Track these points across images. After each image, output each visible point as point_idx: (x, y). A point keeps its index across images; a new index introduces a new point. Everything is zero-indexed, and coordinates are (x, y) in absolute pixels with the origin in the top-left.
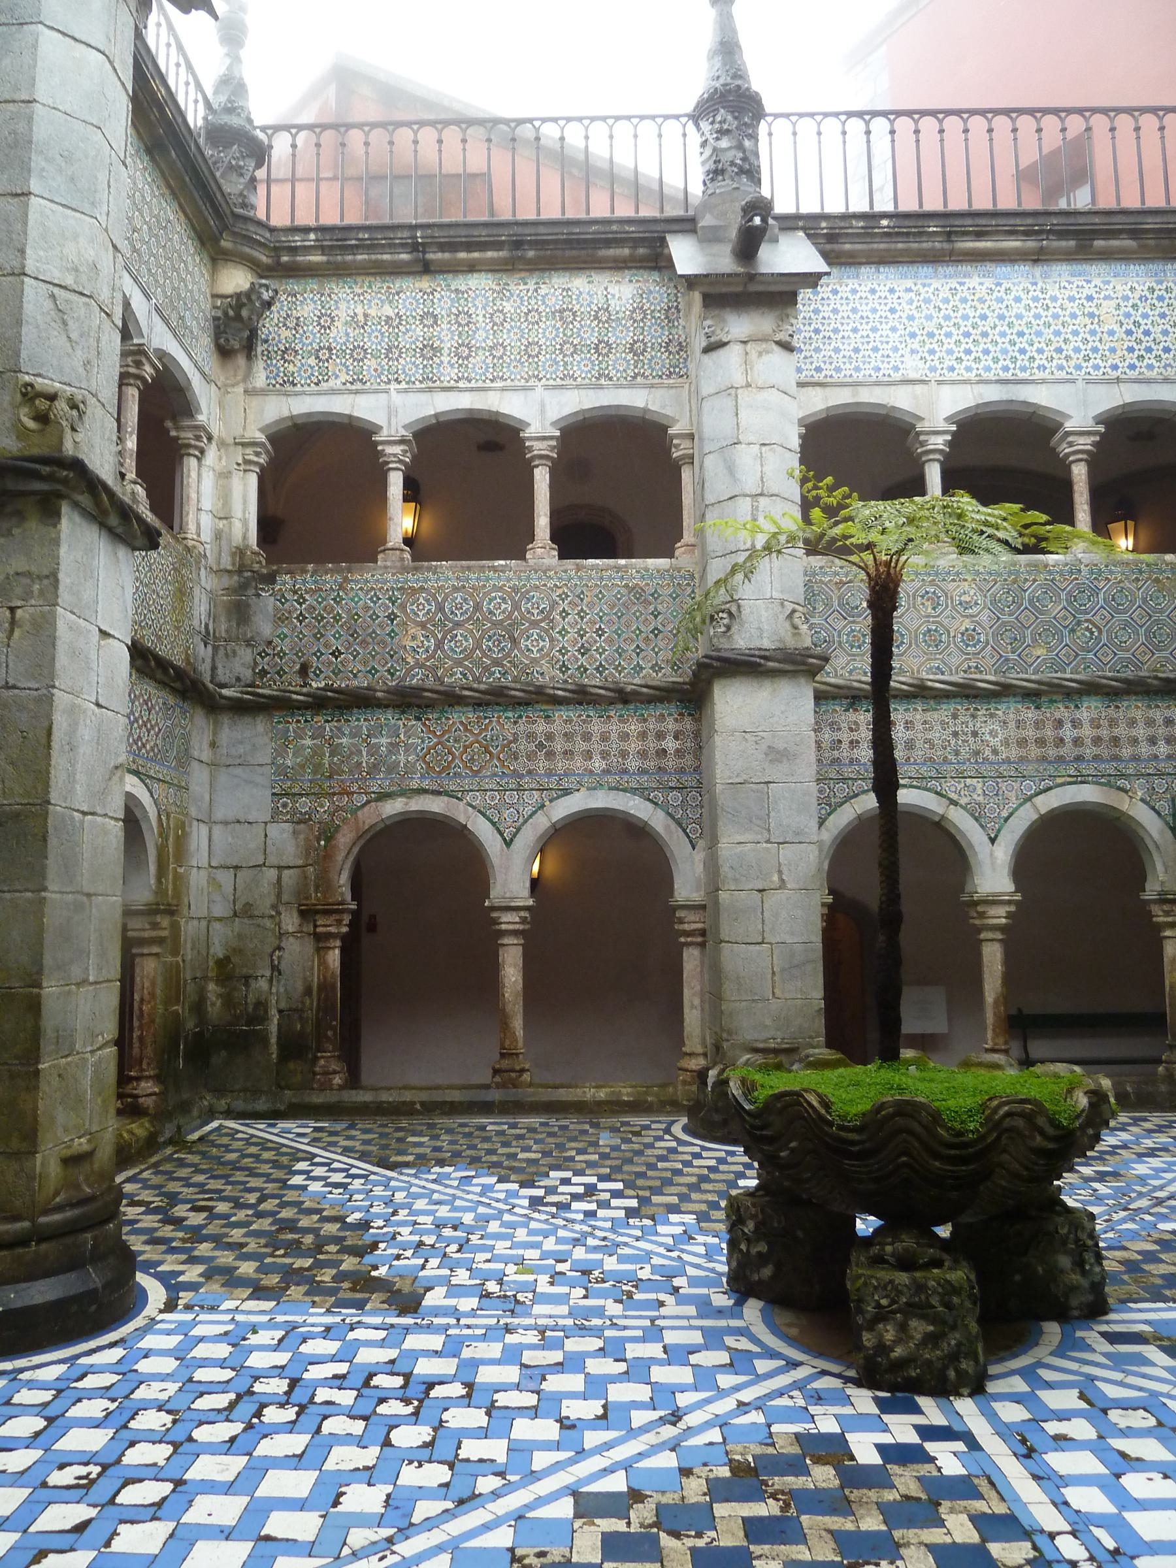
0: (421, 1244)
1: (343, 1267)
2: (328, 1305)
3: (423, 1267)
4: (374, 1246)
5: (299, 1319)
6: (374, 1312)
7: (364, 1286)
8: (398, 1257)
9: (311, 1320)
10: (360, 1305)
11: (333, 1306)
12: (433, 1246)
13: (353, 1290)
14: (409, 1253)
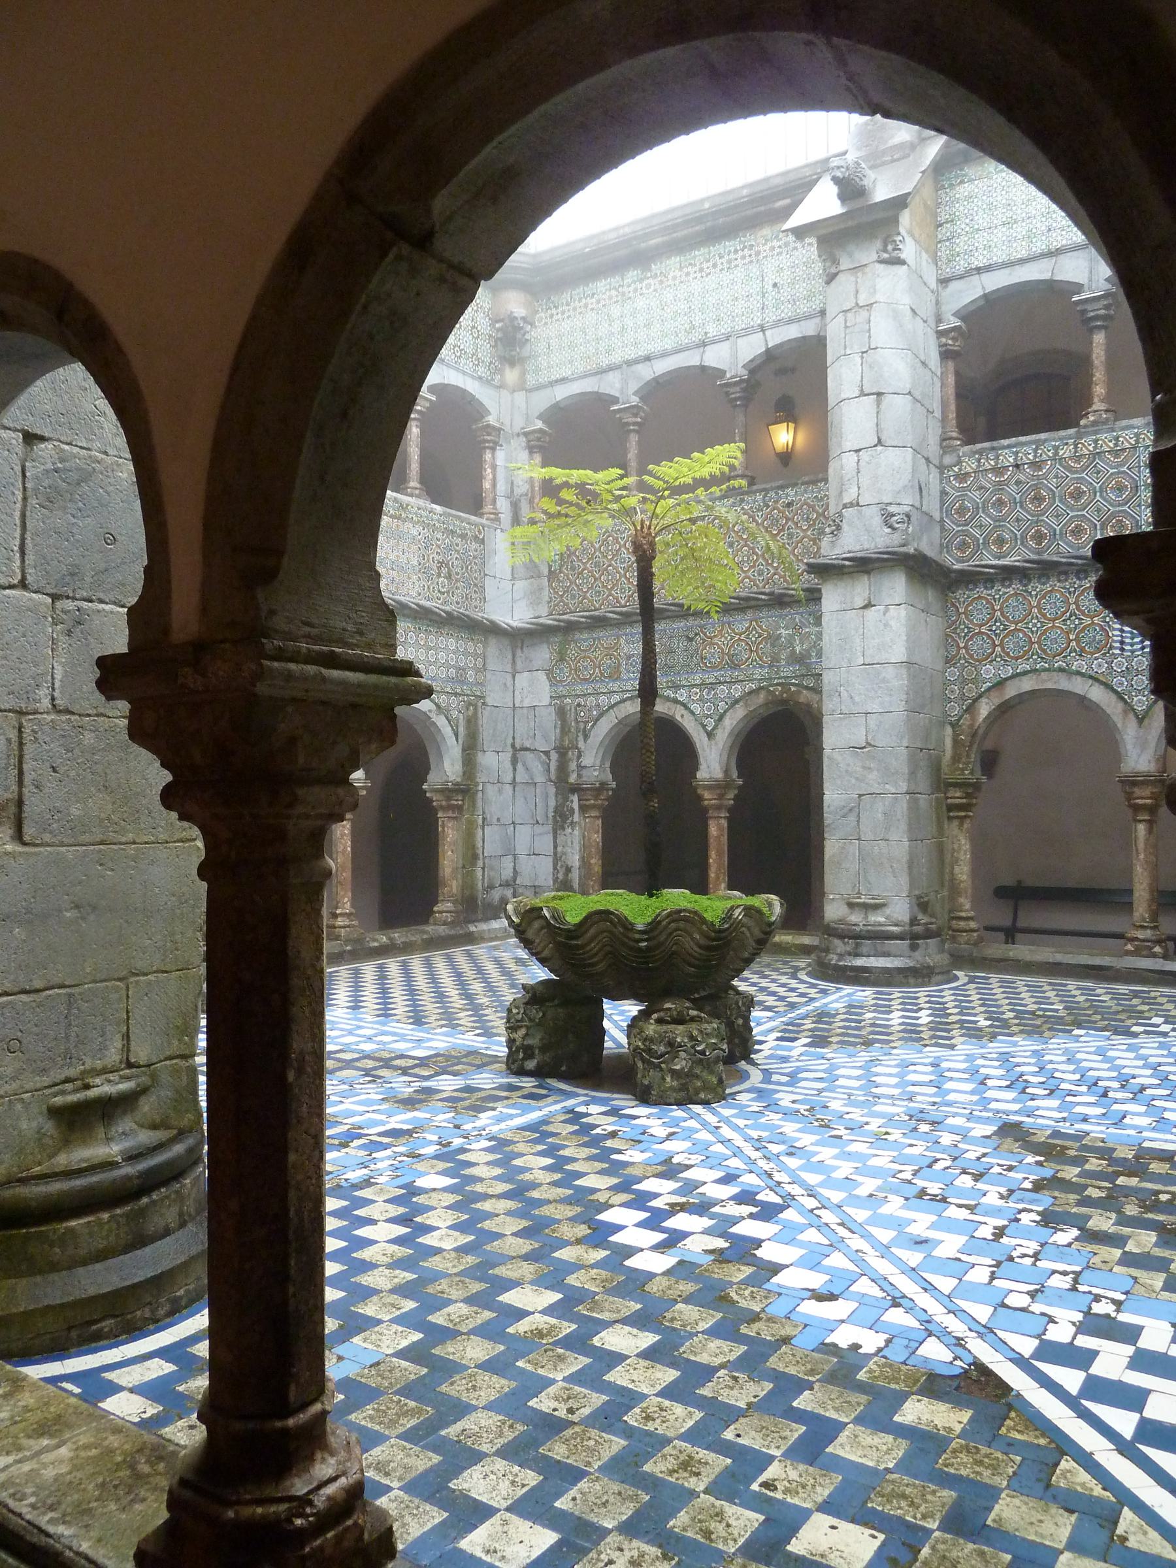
0: (978, 1177)
1: (1077, 1170)
2: (1088, 1138)
3: (984, 1155)
4: (1038, 1187)
5: (1112, 1130)
6: (1043, 1128)
7: (1051, 1150)
8: (1010, 1168)
9: (1103, 1128)
10: (1056, 1134)
11: (1084, 1137)
12: (964, 1172)
13: (1065, 1148)
14: (996, 1169)
